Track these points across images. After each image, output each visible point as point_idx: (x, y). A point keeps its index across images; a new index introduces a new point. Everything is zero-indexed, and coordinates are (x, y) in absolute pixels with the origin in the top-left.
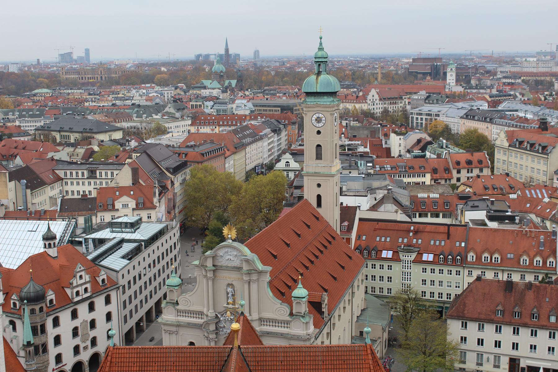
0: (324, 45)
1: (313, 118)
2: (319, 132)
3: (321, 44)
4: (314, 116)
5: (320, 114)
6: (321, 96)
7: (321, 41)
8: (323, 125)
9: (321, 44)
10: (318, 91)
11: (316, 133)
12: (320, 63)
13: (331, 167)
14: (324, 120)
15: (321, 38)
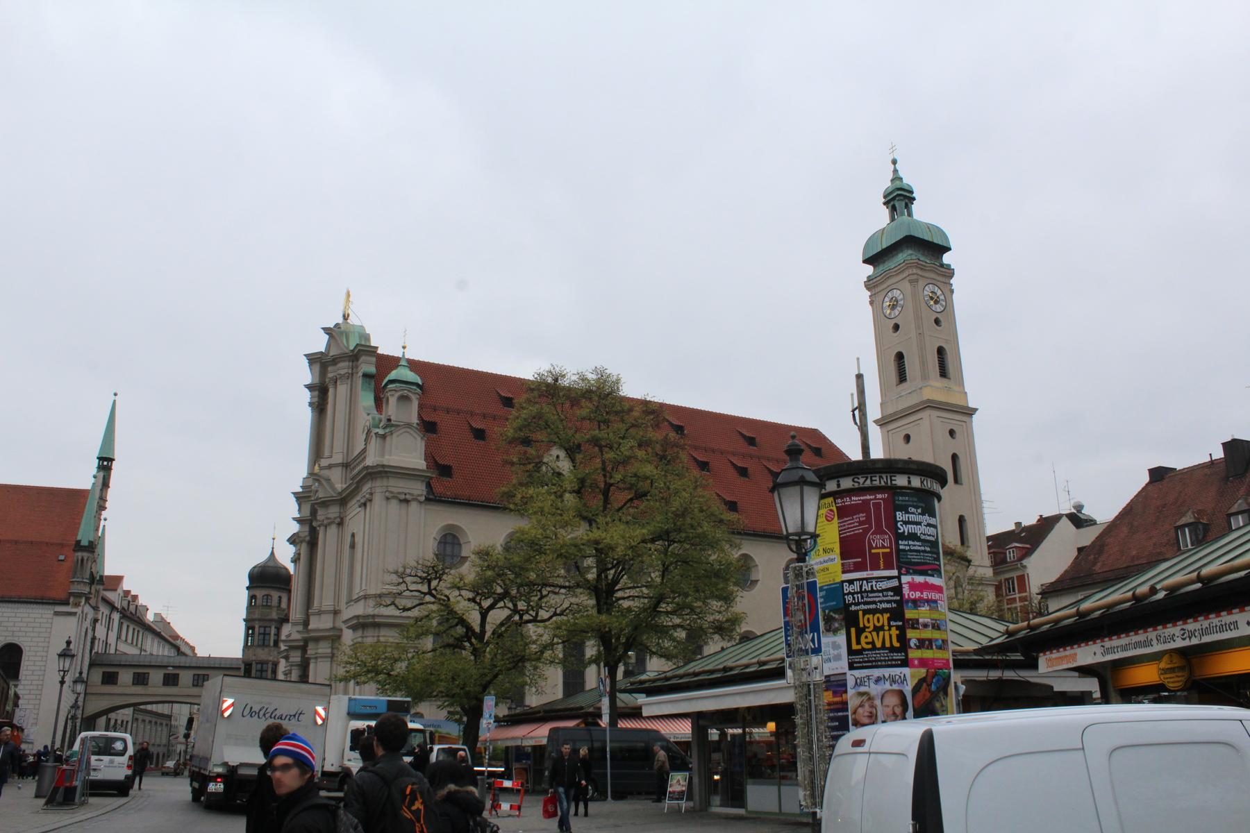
0: (901, 174)
1: (884, 305)
2: (896, 327)
3: (895, 171)
4: (887, 299)
5: (895, 291)
6: (893, 257)
7: (895, 167)
8: (900, 309)
9: (895, 171)
10: (884, 246)
11: (891, 330)
12: (892, 203)
13: (921, 389)
14: (901, 300)
15: (894, 162)
